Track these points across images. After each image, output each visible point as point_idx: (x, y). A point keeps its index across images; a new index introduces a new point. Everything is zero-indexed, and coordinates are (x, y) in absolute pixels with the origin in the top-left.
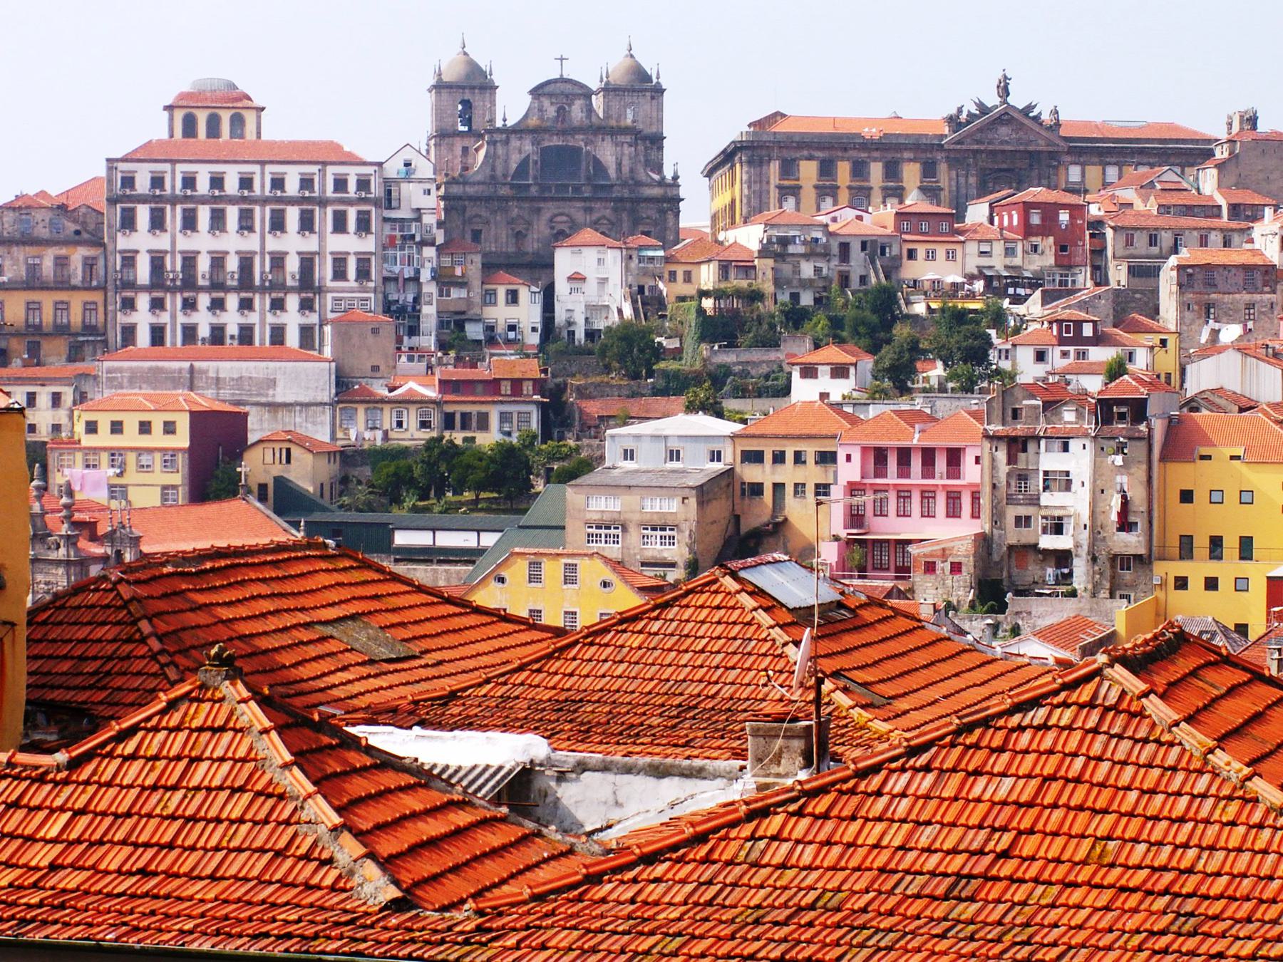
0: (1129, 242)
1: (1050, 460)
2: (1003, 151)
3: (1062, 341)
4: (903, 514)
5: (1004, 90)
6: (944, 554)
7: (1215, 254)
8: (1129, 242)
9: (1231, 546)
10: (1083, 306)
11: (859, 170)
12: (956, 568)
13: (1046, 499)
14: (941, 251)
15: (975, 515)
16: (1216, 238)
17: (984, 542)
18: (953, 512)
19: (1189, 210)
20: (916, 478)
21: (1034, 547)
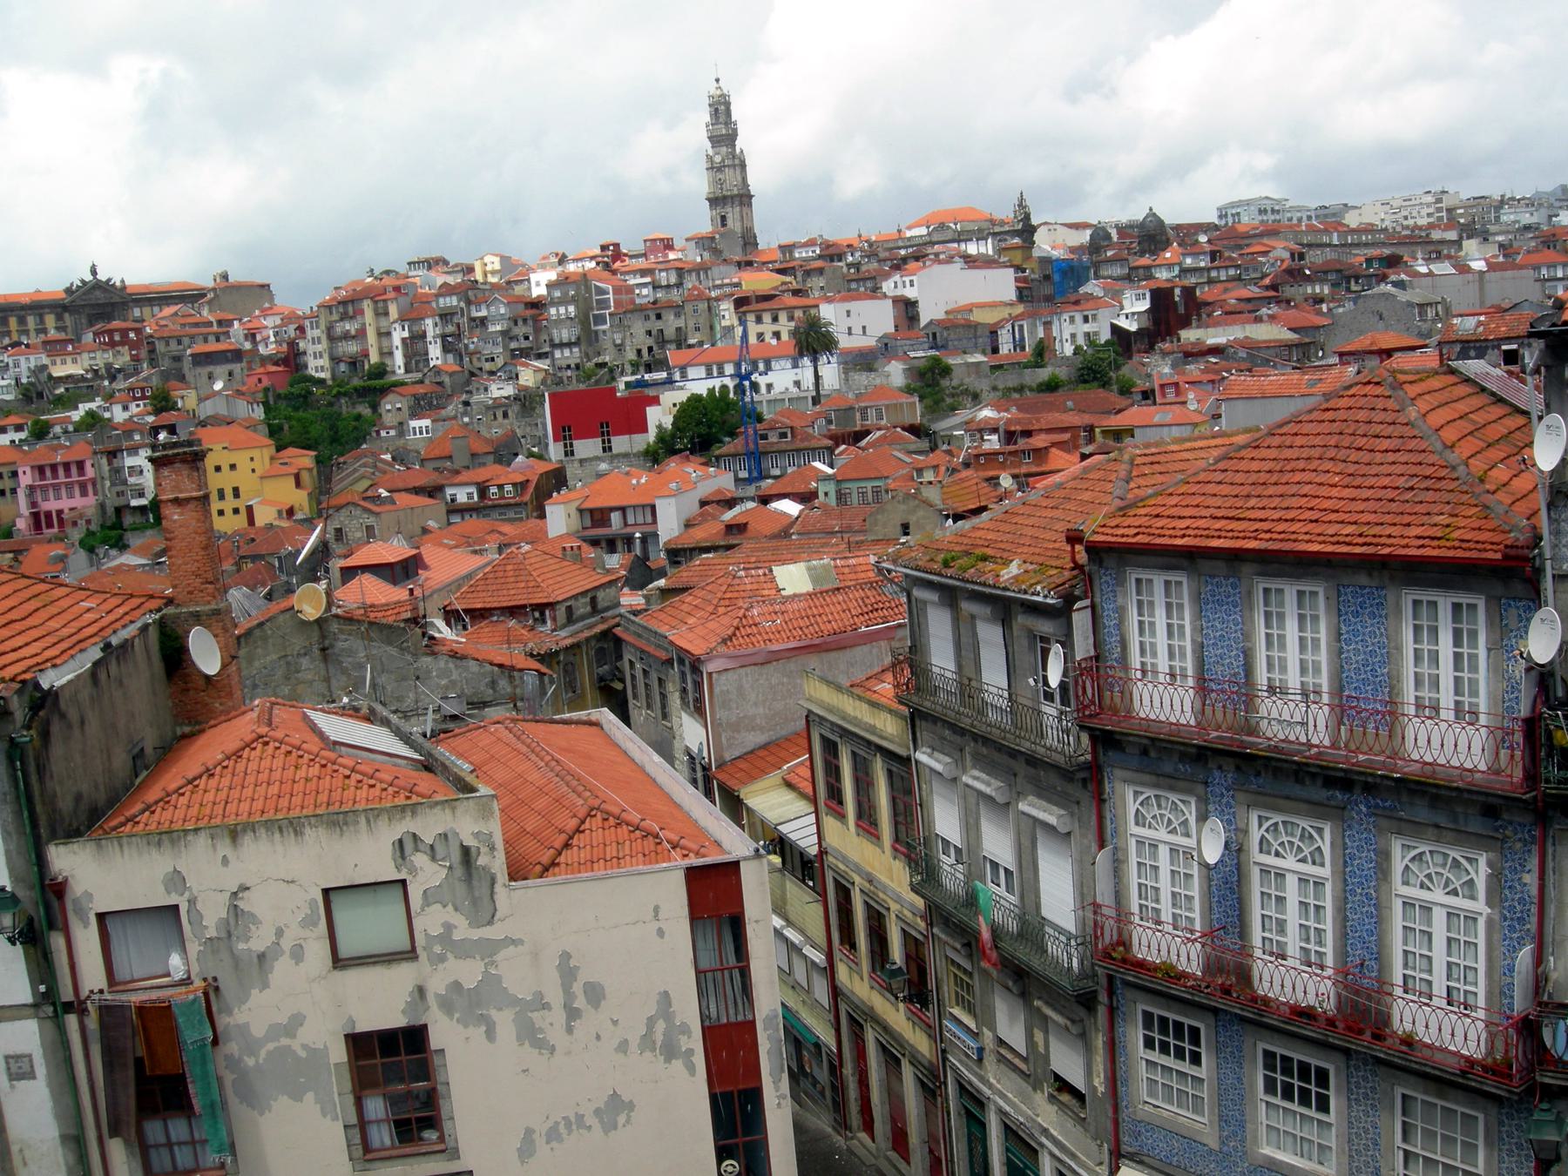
0: (168, 344)
1: (130, 461)
2: (97, 306)
3: (136, 399)
4: (58, 498)
5: (94, 272)
6: (81, 517)
7: (212, 346)
8: (168, 344)
9: (229, 493)
10: (145, 379)
11: (22, 321)
12: (88, 522)
13: (132, 480)
14: (69, 359)
15: (95, 494)
16: (211, 338)
17: (102, 506)
18: (84, 493)
19: (197, 325)
20: (62, 479)
21: (128, 506)
